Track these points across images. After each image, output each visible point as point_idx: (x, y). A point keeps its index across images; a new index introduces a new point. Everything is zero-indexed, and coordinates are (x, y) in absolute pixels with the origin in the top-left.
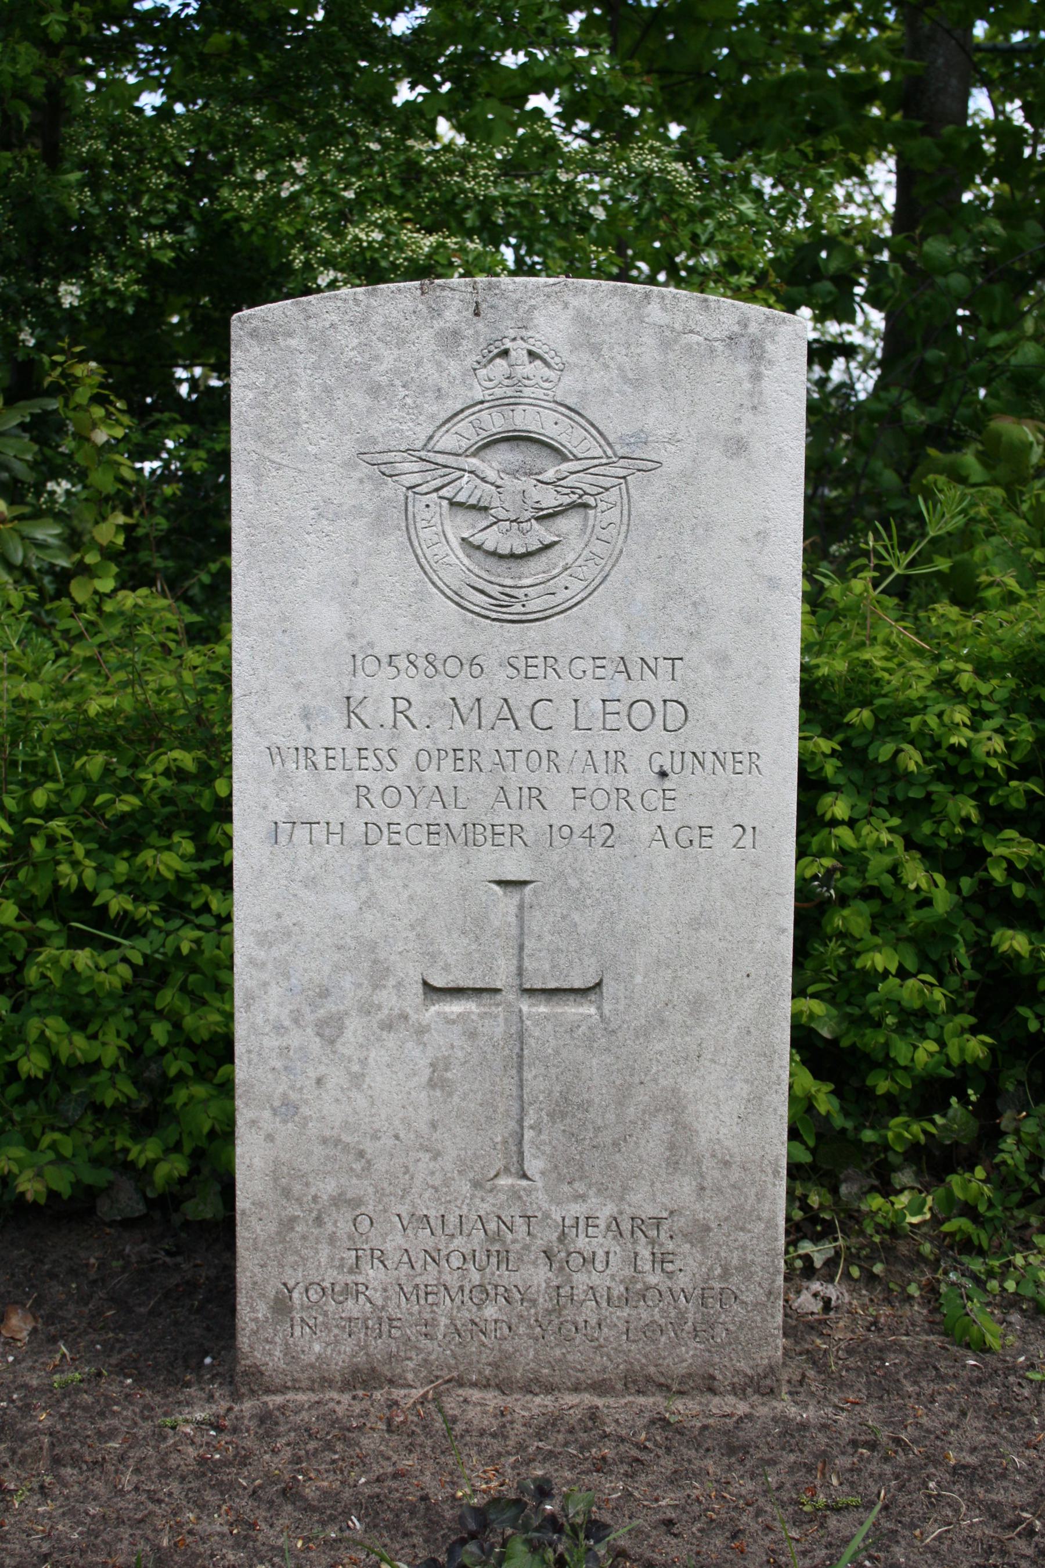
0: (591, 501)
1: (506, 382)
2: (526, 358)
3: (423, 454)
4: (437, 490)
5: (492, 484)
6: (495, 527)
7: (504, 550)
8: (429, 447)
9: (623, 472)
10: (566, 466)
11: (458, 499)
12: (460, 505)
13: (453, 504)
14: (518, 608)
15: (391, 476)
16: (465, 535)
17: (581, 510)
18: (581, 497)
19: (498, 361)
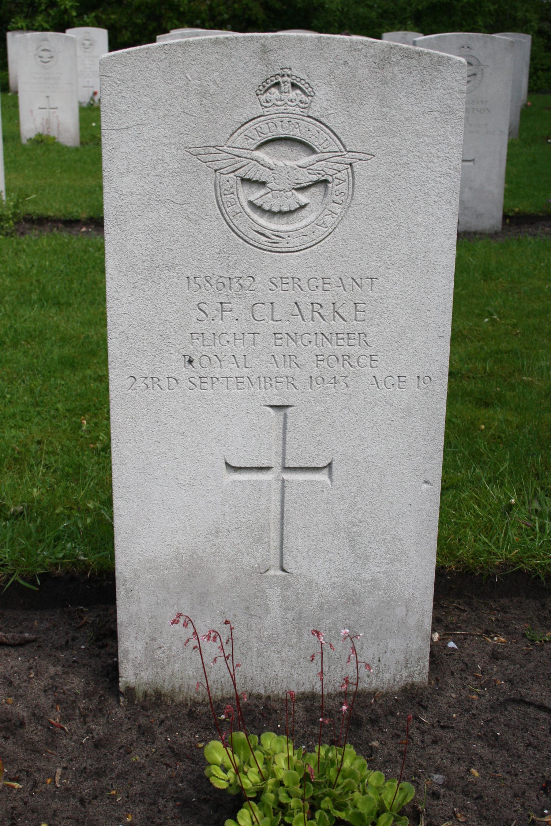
0: (330, 179)
1: (279, 103)
2: (290, 89)
4: (234, 172)
5: (269, 168)
6: (270, 194)
7: (276, 209)
8: (229, 143)
9: (349, 161)
10: (314, 157)
13: (243, 180)
14: (283, 244)
15: (205, 162)
16: (251, 198)
18: (323, 176)
19: (273, 90)
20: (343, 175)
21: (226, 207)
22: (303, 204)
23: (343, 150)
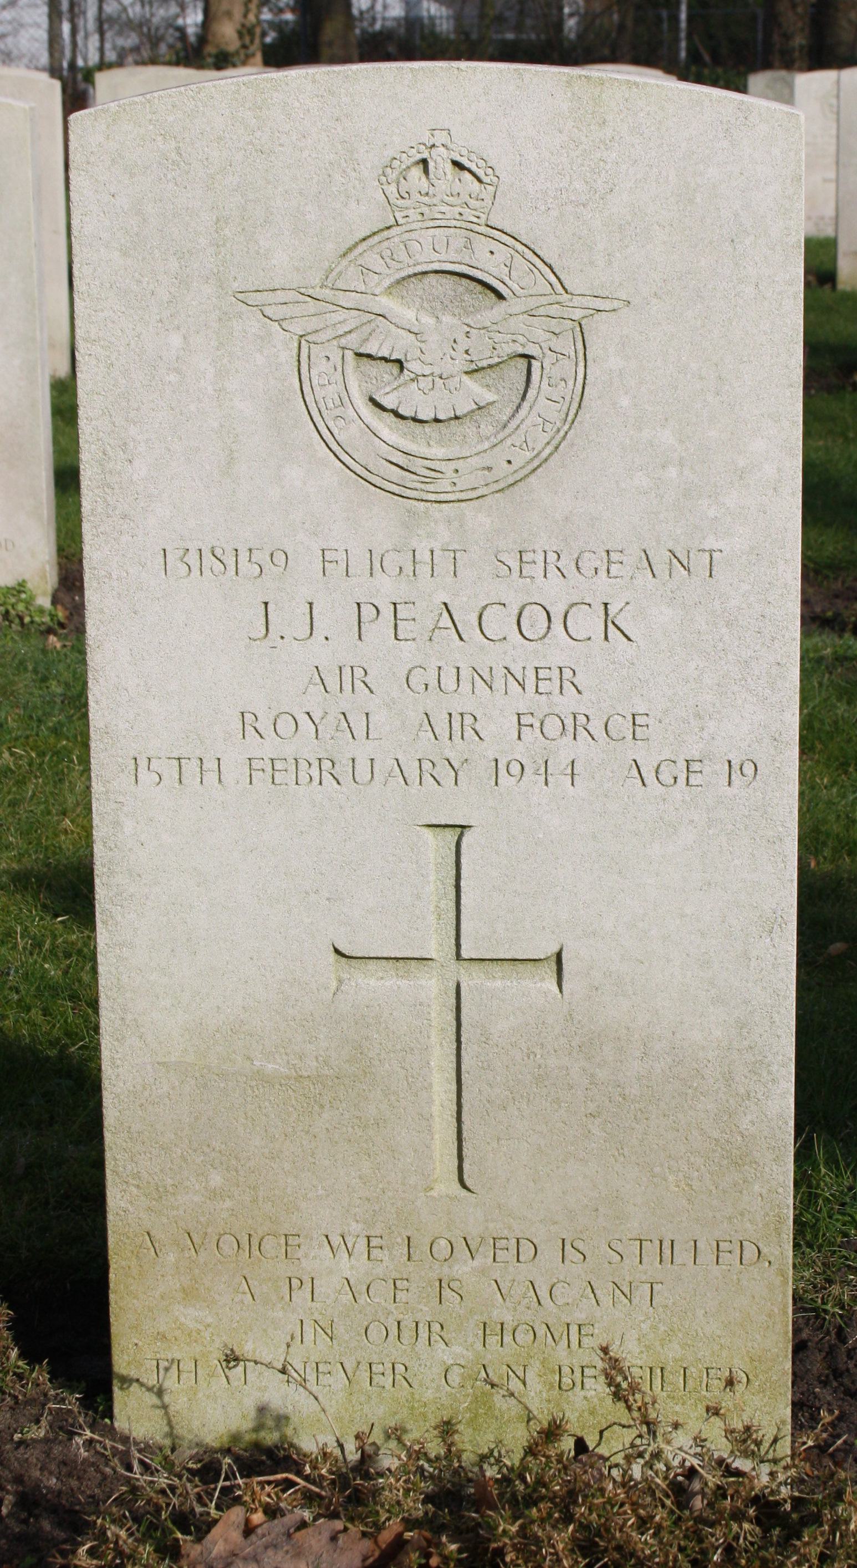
3: (316, 292)
11: (362, 351)
12: (369, 356)
14: (444, 485)
17: (522, 363)
20: (565, 345)
21: (323, 409)
22: (481, 404)
23: (561, 291)
